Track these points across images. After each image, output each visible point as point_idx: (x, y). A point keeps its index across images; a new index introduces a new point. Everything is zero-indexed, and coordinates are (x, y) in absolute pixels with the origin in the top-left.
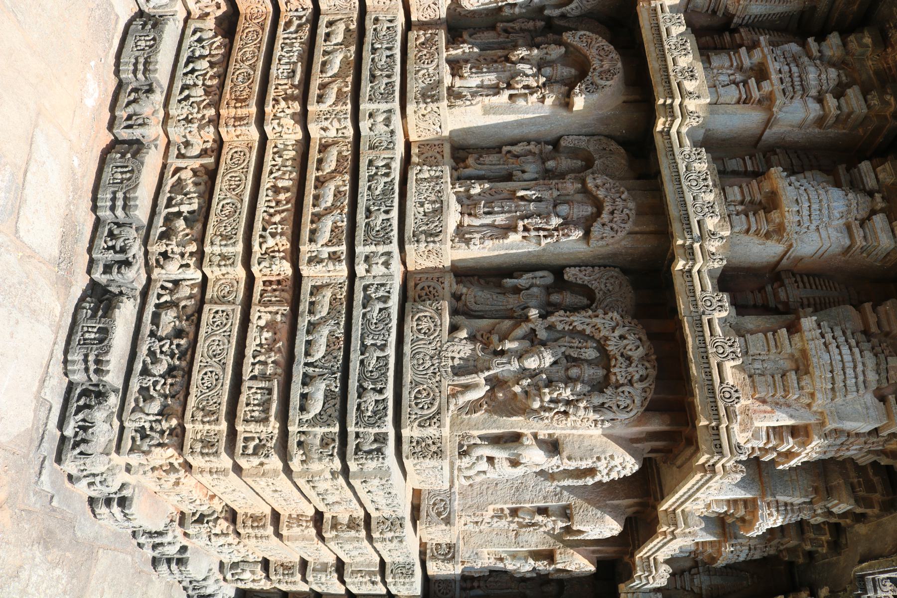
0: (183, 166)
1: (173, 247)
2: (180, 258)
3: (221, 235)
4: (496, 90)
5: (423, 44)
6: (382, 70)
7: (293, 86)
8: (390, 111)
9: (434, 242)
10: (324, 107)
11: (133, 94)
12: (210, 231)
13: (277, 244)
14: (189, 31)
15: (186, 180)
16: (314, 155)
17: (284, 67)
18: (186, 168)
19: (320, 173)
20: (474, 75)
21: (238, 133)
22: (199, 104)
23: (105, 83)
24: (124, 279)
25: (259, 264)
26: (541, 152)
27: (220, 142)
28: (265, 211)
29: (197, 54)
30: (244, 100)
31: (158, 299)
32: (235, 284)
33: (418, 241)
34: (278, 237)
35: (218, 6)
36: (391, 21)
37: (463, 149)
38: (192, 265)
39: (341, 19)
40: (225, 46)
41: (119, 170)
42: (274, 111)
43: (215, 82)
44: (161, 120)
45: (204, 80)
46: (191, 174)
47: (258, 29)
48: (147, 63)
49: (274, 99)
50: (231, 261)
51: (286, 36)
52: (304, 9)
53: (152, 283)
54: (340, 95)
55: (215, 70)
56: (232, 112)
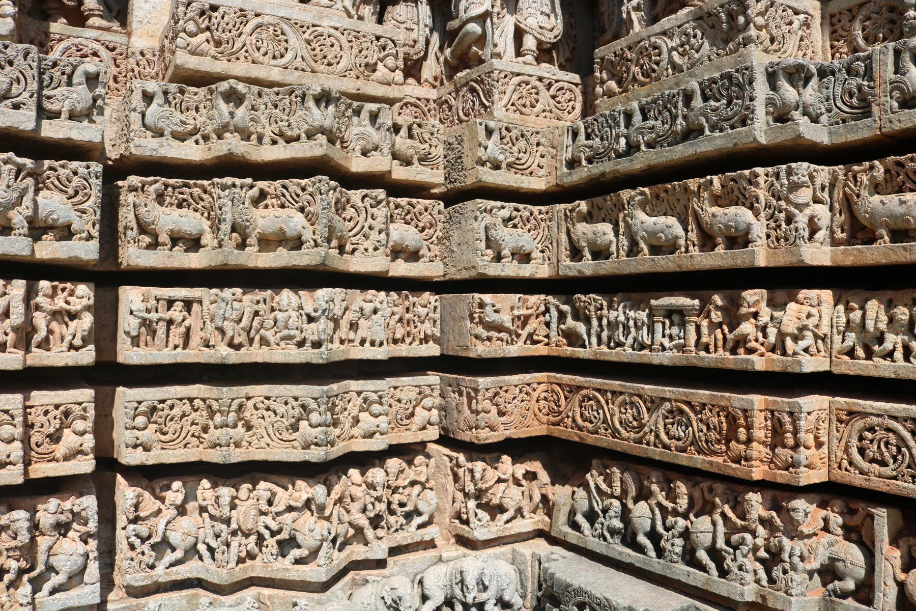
5: (620, 83)
6: (674, 118)
7: (703, 311)
8: (772, 78)
10: (759, 228)
14: (572, 536)
21: (811, 442)
27: (826, 492)
29: (617, 524)
30: (732, 420)
35: (531, 476)
36: (575, 134)
39: (568, 233)
42: (763, 349)
43: (682, 488)
47: (577, 398)
49: (734, 351)
51: (594, 340)
52: (548, 310)
54: (732, 197)
55: (655, 488)
56: (758, 450)
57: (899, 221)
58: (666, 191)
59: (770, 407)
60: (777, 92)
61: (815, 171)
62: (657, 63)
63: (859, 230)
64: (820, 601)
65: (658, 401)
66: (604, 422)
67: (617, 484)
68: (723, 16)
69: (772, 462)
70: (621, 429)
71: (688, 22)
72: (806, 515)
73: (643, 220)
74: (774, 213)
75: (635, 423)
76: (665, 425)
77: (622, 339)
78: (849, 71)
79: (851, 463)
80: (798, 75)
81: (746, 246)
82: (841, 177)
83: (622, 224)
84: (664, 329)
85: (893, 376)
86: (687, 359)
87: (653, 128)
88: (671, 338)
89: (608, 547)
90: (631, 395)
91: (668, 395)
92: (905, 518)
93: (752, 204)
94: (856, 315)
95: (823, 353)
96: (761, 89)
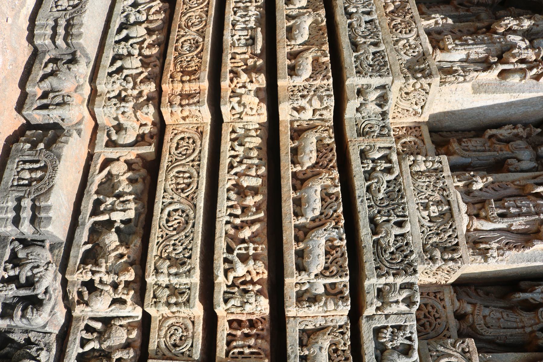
0: (114, 156)
1: (103, 276)
2: (111, 291)
3: (169, 258)
4: (485, 65)
5: (392, 12)
6: (365, 37)
8: (383, 87)
9: (452, 259)
10: (299, 81)
11: (51, 65)
12: (153, 251)
13: (249, 272)
15: (118, 176)
16: (286, 143)
17: (240, 33)
18: (118, 159)
19: (298, 168)
20: (459, 48)
21: (186, 113)
22: (134, 77)
23: (14, 50)
24: (30, 324)
25: (226, 301)
26: (529, 135)
27: (161, 125)
28: (228, 223)
29: (132, 19)
30: (194, 72)
31: (82, 346)
32: (190, 326)
33: (431, 259)
34: (251, 262)
37: (450, 131)
38: (129, 302)
40: (165, 11)
41: (28, 166)
42: (233, 86)
43: (155, 51)
44: (87, 98)
45: (141, 49)
46: (125, 167)
48: (69, 26)
49: (231, 71)
50: (185, 297)
53: (74, 323)
55: (154, 37)
56: (178, 87)
57: (302, 150)
58: (323, 34)
59: (201, 92)
60: (374, 89)
61: (330, 110)
62: (401, 32)
63: (298, 133)
64: (104, 124)
65: (203, 35)
66: (190, 7)
67: (155, 17)
68: (423, 66)
69: (172, 95)
70: (186, 16)
71: (422, 48)
72: (147, 114)
73: (307, 22)
74: (307, 89)
75: (190, 24)
76: (189, 40)
77: (238, 14)
78: (383, 127)
79: (176, 134)
80: (382, 101)
81: (289, 75)
82: (327, 124)
83: (305, 11)
84: (244, 36)
85: (221, 150)
86: (227, 48)
87: (360, 26)
88: (239, 40)
89: (118, 14)
90: (206, 21)
91: (206, 39)
92: (152, 161)
93: (312, 78)
94: (253, 133)
95: (232, 118)
96: (376, 81)
